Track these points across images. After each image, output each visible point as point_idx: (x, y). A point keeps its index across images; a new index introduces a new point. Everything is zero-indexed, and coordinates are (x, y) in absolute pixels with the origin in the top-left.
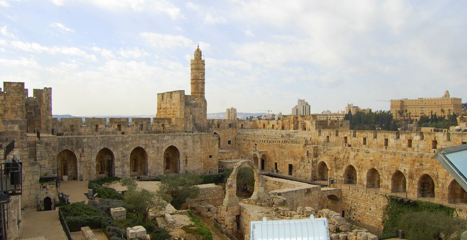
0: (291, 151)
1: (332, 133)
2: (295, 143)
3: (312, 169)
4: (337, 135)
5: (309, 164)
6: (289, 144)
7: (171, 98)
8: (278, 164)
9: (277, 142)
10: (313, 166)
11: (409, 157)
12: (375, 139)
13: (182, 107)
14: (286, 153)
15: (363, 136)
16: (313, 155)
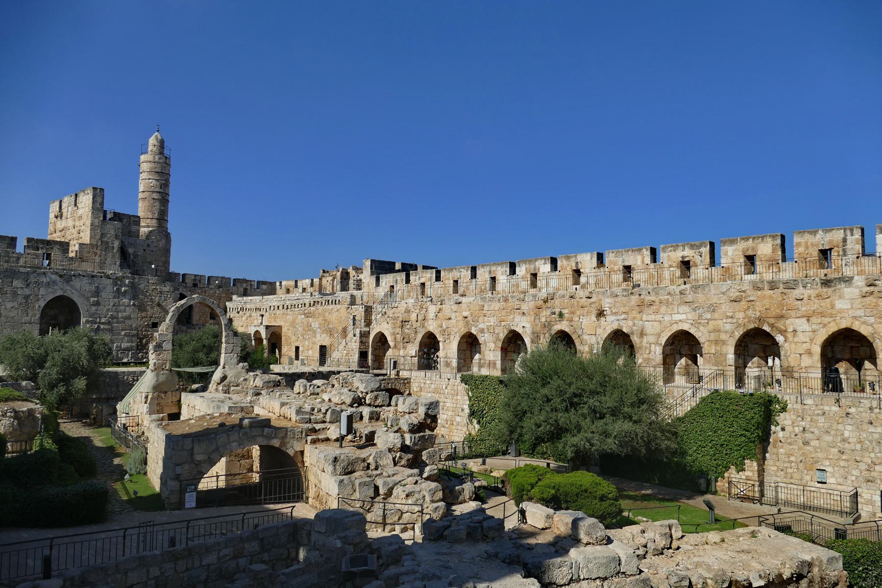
0: (324, 320)
1: (399, 279)
2: (332, 304)
3: (360, 348)
4: (408, 281)
5: (355, 338)
6: (322, 307)
7: (76, 205)
8: (301, 349)
9: (300, 306)
10: (361, 342)
11: (531, 301)
12: (474, 280)
13: (97, 220)
14: (315, 325)
15: (453, 278)
16: (365, 322)
